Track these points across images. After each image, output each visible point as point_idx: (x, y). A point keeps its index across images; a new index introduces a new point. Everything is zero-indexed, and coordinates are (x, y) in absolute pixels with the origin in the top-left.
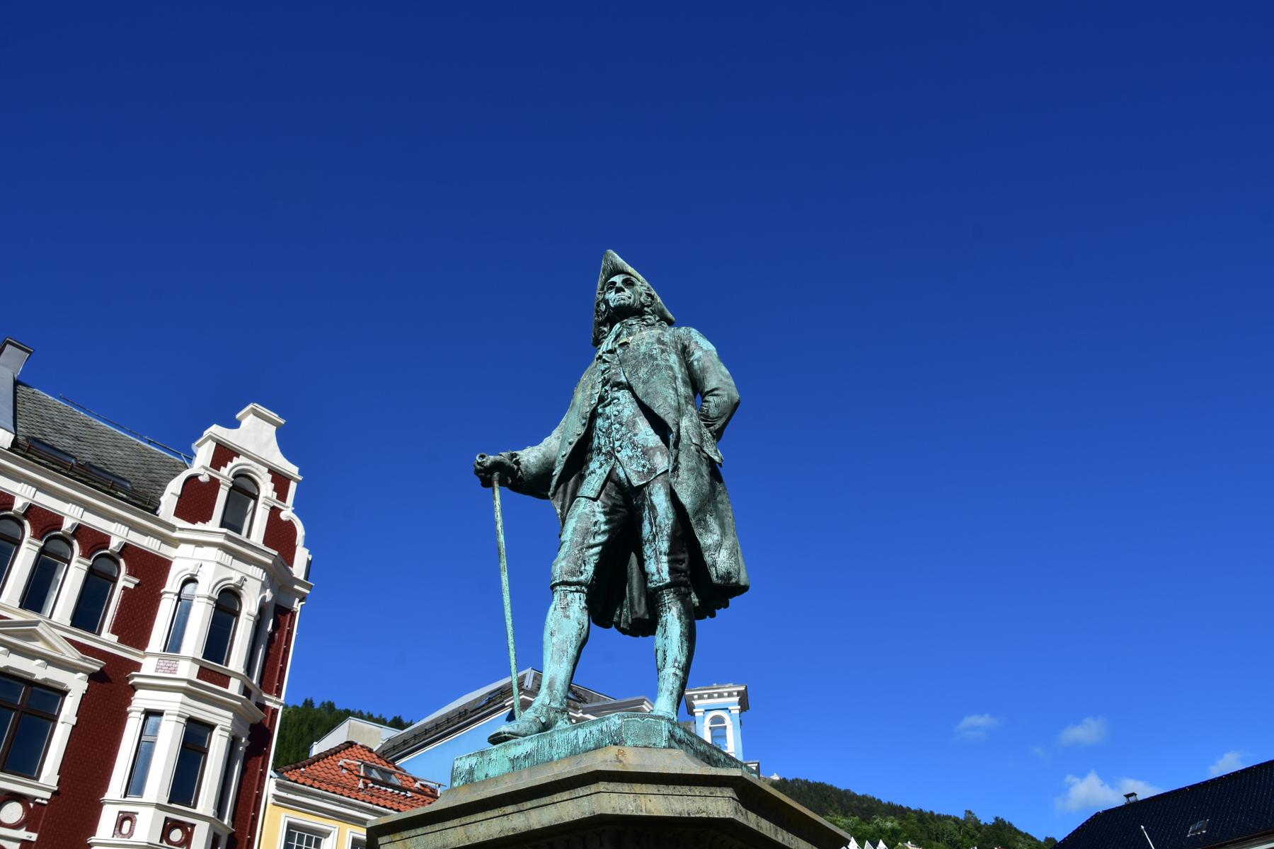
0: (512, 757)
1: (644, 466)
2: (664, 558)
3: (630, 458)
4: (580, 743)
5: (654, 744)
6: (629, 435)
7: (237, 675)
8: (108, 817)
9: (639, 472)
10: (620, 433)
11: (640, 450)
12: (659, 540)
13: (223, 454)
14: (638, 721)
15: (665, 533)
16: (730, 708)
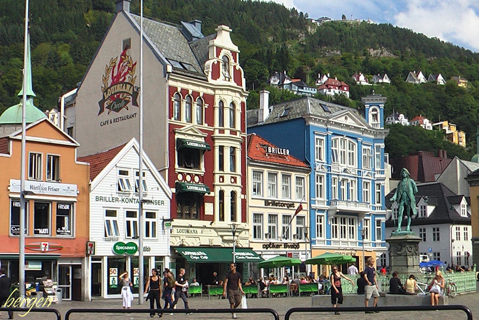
7: (238, 131)
8: (217, 177)
13: (219, 50)
16: (380, 105)
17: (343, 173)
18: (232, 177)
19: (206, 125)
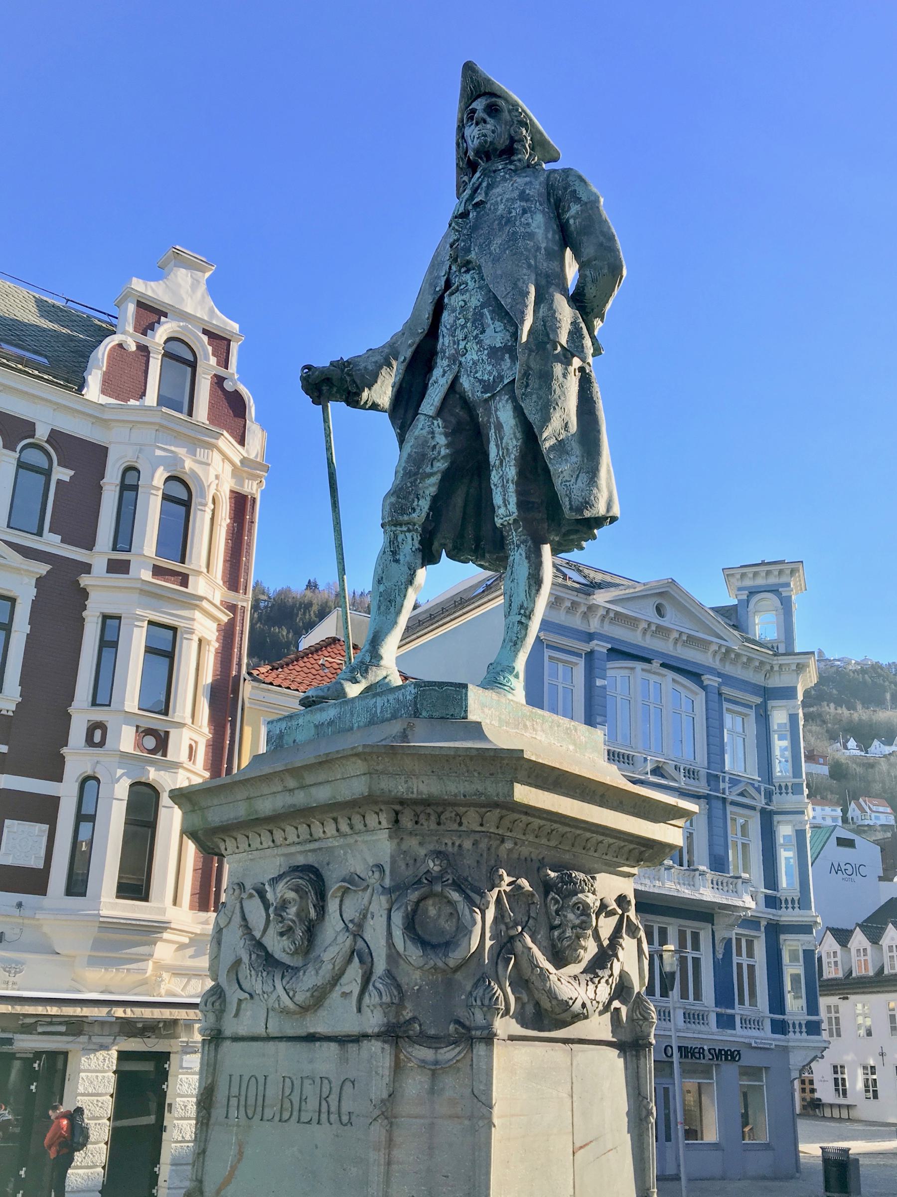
0: (317, 723)
1: (490, 373)
2: (512, 488)
3: (475, 363)
4: (378, 712)
5: (452, 715)
6: (475, 333)
9: (485, 381)
10: (466, 330)
11: (486, 352)
12: (506, 465)
14: (435, 690)
15: (513, 456)
17: (649, 776)
18: (149, 732)
19: (58, 538)
